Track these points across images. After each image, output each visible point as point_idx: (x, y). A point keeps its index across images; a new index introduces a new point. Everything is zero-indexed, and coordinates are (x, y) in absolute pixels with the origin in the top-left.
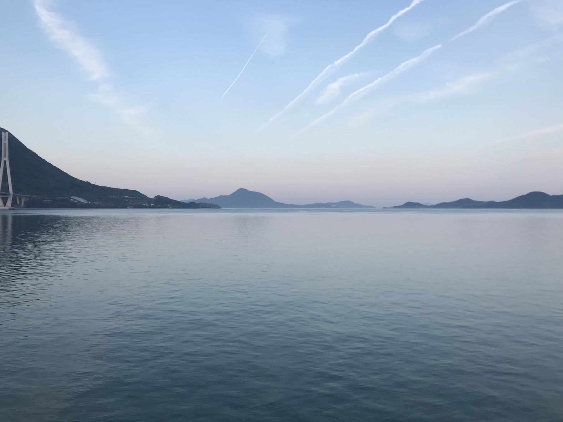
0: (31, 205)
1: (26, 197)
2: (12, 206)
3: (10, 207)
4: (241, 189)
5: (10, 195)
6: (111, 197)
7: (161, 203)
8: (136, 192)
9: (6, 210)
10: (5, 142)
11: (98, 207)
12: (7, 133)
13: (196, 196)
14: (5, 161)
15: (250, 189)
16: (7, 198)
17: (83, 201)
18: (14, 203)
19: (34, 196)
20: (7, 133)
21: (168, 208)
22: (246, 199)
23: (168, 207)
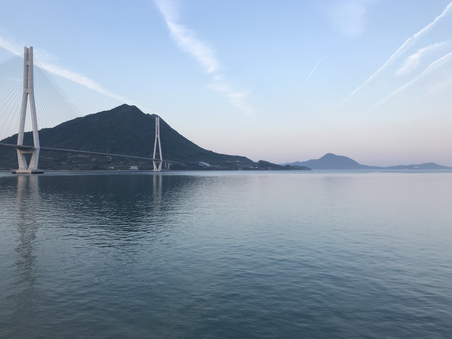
0: (173, 168)
1: (171, 162)
4: (329, 154)
5: (160, 161)
6: (227, 162)
7: (264, 166)
8: (244, 158)
9: (158, 171)
10: (158, 124)
11: (218, 169)
12: (158, 118)
13: (291, 161)
15: (337, 154)
16: (159, 163)
18: (163, 167)
20: (158, 118)
22: (333, 162)
23: (267, 169)
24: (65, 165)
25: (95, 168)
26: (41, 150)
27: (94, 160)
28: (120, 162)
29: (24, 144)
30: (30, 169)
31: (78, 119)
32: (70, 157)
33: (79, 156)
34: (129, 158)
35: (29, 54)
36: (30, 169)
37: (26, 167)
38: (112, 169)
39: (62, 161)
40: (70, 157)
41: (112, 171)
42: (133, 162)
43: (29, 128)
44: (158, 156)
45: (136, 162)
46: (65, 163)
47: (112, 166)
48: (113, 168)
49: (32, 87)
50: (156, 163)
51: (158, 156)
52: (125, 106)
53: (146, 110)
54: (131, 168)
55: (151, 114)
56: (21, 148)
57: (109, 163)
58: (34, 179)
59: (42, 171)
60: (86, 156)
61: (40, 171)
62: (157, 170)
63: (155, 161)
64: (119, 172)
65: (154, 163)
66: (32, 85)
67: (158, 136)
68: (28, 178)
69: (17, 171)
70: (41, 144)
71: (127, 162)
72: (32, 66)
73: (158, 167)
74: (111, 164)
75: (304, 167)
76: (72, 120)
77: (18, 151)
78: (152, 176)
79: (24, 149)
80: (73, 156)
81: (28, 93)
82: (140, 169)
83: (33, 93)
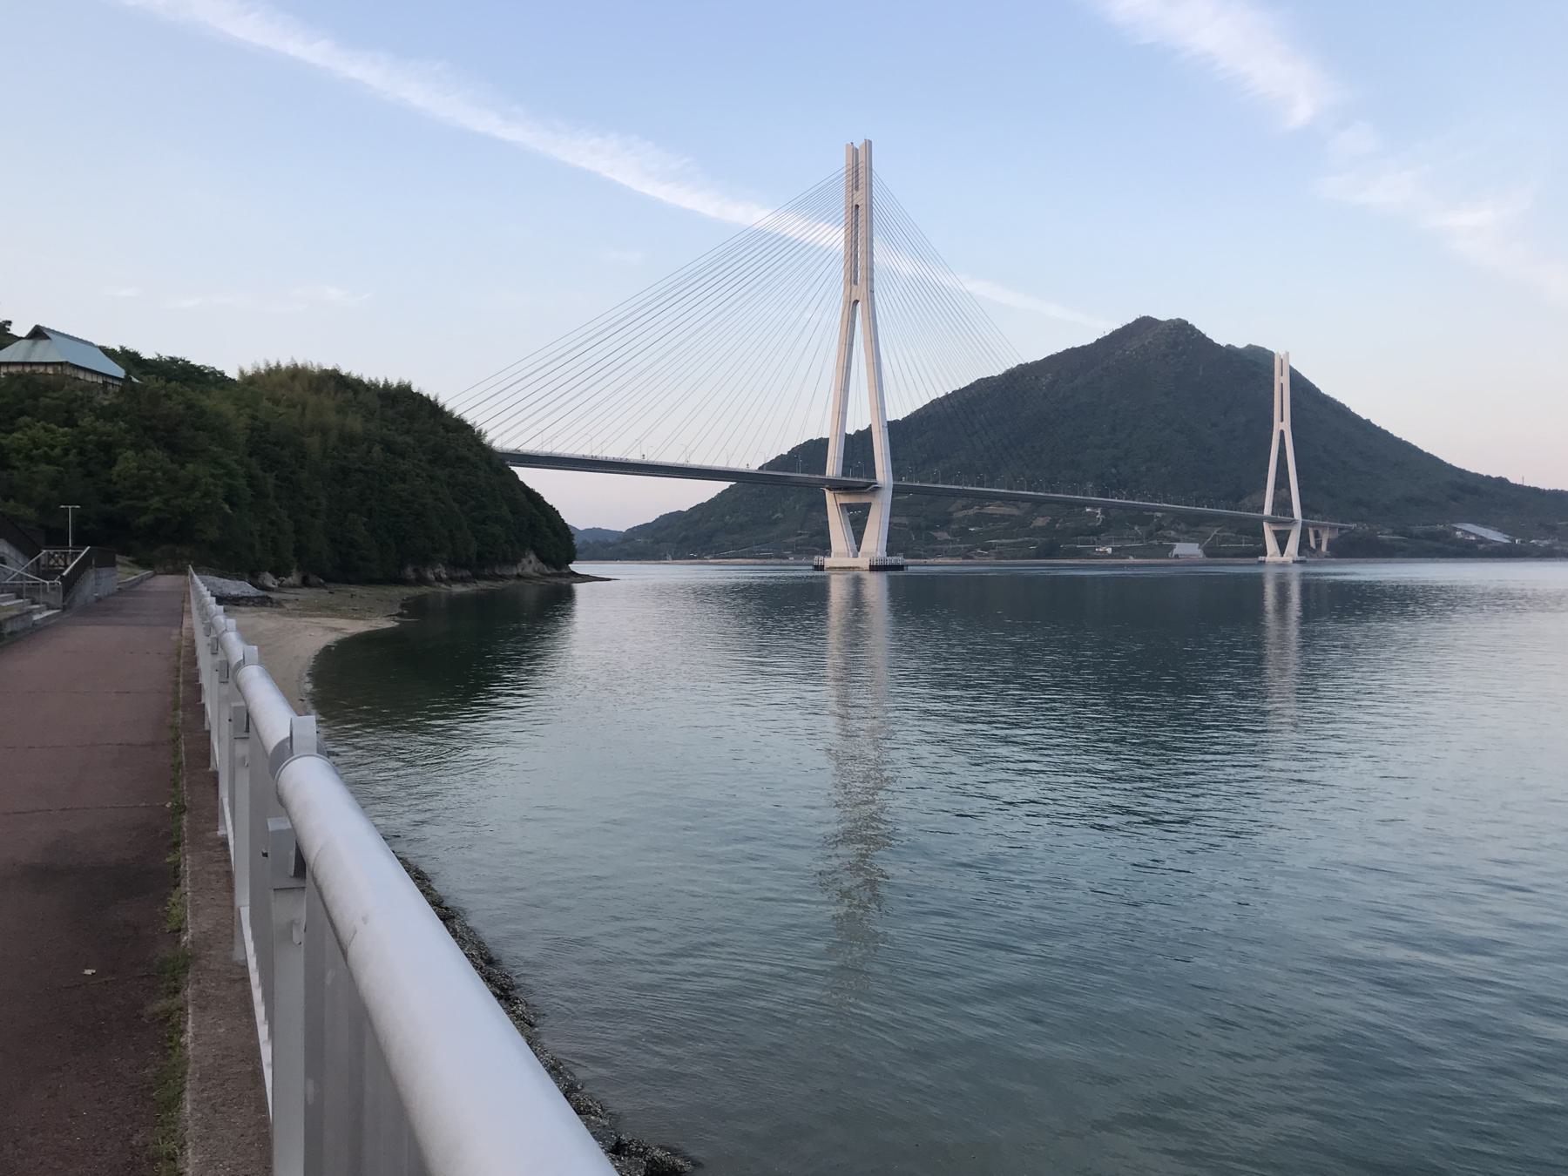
3: (1297, 558)
5: (1293, 522)
9: (1284, 564)
10: (1282, 381)
14: (1282, 433)
16: (1287, 534)
18: (1303, 546)
19: (1353, 526)
24: (946, 542)
25: (1050, 551)
26: (896, 491)
27: (1040, 522)
29: (844, 474)
33: (991, 509)
35: (859, 171)
36: (865, 554)
37: (854, 551)
38: (1105, 555)
39: (936, 529)
40: (960, 514)
41: (1105, 562)
42: (1183, 527)
44: (1283, 505)
45: (1192, 526)
47: (1106, 543)
48: (1109, 550)
49: (870, 280)
50: (1276, 533)
51: (1283, 505)
52: (1145, 324)
53: (1226, 330)
54: (1176, 551)
56: (838, 487)
57: (1096, 532)
58: (876, 589)
59: (899, 559)
60: (1015, 512)
61: (892, 560)
62: (1279, 559)
63: (1272, 521)
64: (1134, 565)
65: (1268, 530)
66: (870, 269)
67: (1282, 425)
68: (857, 582)
69: (829, 562)
70: (897, 473)
71: (1161, 527)
73: (1282, 546)
76: (961, 391)
77: (829, 495)
78: (1257, 582)
79: (846, 489)
80: (971, 512)
82: (1210, 552)
83: (873, 299)
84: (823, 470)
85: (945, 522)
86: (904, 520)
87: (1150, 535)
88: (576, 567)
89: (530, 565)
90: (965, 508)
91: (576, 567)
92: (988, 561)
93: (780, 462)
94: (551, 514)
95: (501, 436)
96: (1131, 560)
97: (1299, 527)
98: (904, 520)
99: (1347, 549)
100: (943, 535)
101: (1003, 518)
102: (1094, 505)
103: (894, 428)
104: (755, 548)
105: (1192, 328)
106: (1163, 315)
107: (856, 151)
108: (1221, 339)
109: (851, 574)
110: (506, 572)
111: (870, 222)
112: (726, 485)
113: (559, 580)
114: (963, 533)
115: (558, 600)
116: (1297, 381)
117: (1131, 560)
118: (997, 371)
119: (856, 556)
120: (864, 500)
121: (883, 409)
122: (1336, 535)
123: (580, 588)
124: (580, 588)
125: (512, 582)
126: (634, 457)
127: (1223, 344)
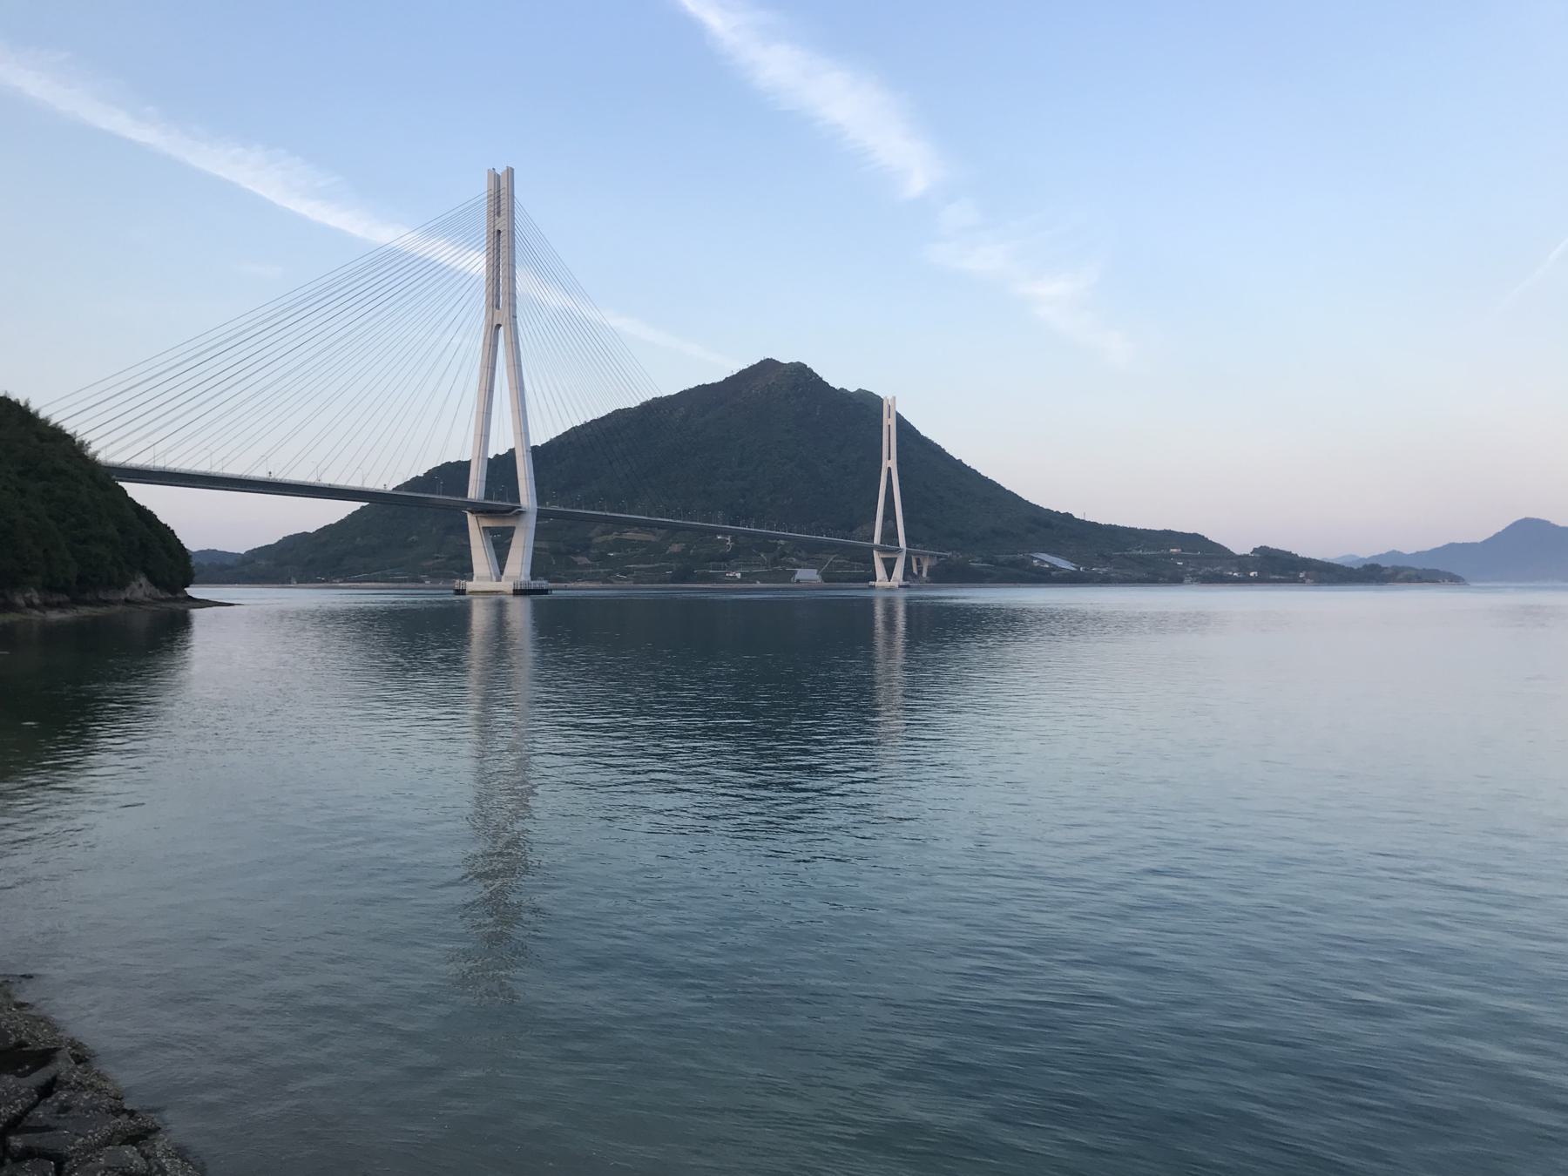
2: (905, 579)
4: (1527, 521)
5: (899, 551)
7: (1276, 568)
9: (891, 589)
10: (889, 422)
11: (1105, 581)
16: (895, 560)
17: (1065, 565)
21: (1303, 581)
24: (587, 566)
25: (683, 576)
27: (675, 548)
28: (752, 559)
30: (508, 578)
31: (618, 413)
32: (600, 539)
33: (629, 535)
34: (795, 538)
36: (508, 578)
37: (497, 574)
39: (576, 554)
40: (600, 539)
41: (737, 586)
42: (803, 554)
43: (499, 446)
44: (890, 535)
45: (811, 554)
46: (585, 560)
47: (735, 569)
48: (739, 575)
49: (512, 305)
50: (885, 561)
51: (890, 535)
52: (768, 365)
53: (840, 375)
54: (797, 576)
55: (852, 389)
56: (480, 510)
57: (725, 558)
58: (520, 613)
60: (653, 538)
62: (888, 584)
63: (881, 550)
64: (762, 591)
66: (512, 295)
67: (890, 463)
68: (501, 607)
69: (470, 586)
70: (541, 497)
71: (784, 554)
72: (512, 233)
73: (890, 572)
74: (733, 563)
75: (1437, 571)
78: (868, 604)
79: (489, 512)
80: (610, 538)
81: (499, 326)
84: (466, 495)
85: (586, 548)
86: (544, 545)
87: (775, 562)
88: (194, 591)
89: (141, 588)
90: (604, 533)
91: (194, 591)
92: (626, 584)
93: (415, 484)
94: (166, 533)
95: (108, 449)
96: (759, 584)
97: (904, 554)
98: (544, 545)
99: (944, 575)
100: (582, 560)
101: (641, 543)
102: (725, 533)
103: (535, 450)
104: (388, 572)
105: (810, 371)
106: (785, 359)
107: (497, 178)
108: (836, 383)
109: (494, 598)
110: (111, 596)
111: (512, 248)
112: (356, 506)
113: (171, 605)
114: (602, 558)
115: (172, 628)
116: (902, 423)
117: (759, 584)
118: (634, 403)
119: (499, 580)
120: (508, 523)
121: (526, 434)
122: (934, 562)
123: (198, 614)
124: (198, 614)
125: (119, 608)
126: (260, 474)
127: (837, 387)
